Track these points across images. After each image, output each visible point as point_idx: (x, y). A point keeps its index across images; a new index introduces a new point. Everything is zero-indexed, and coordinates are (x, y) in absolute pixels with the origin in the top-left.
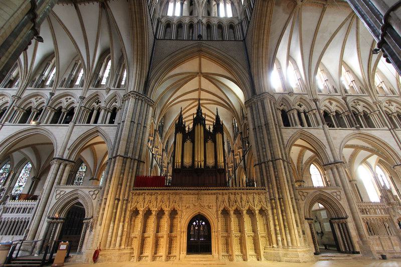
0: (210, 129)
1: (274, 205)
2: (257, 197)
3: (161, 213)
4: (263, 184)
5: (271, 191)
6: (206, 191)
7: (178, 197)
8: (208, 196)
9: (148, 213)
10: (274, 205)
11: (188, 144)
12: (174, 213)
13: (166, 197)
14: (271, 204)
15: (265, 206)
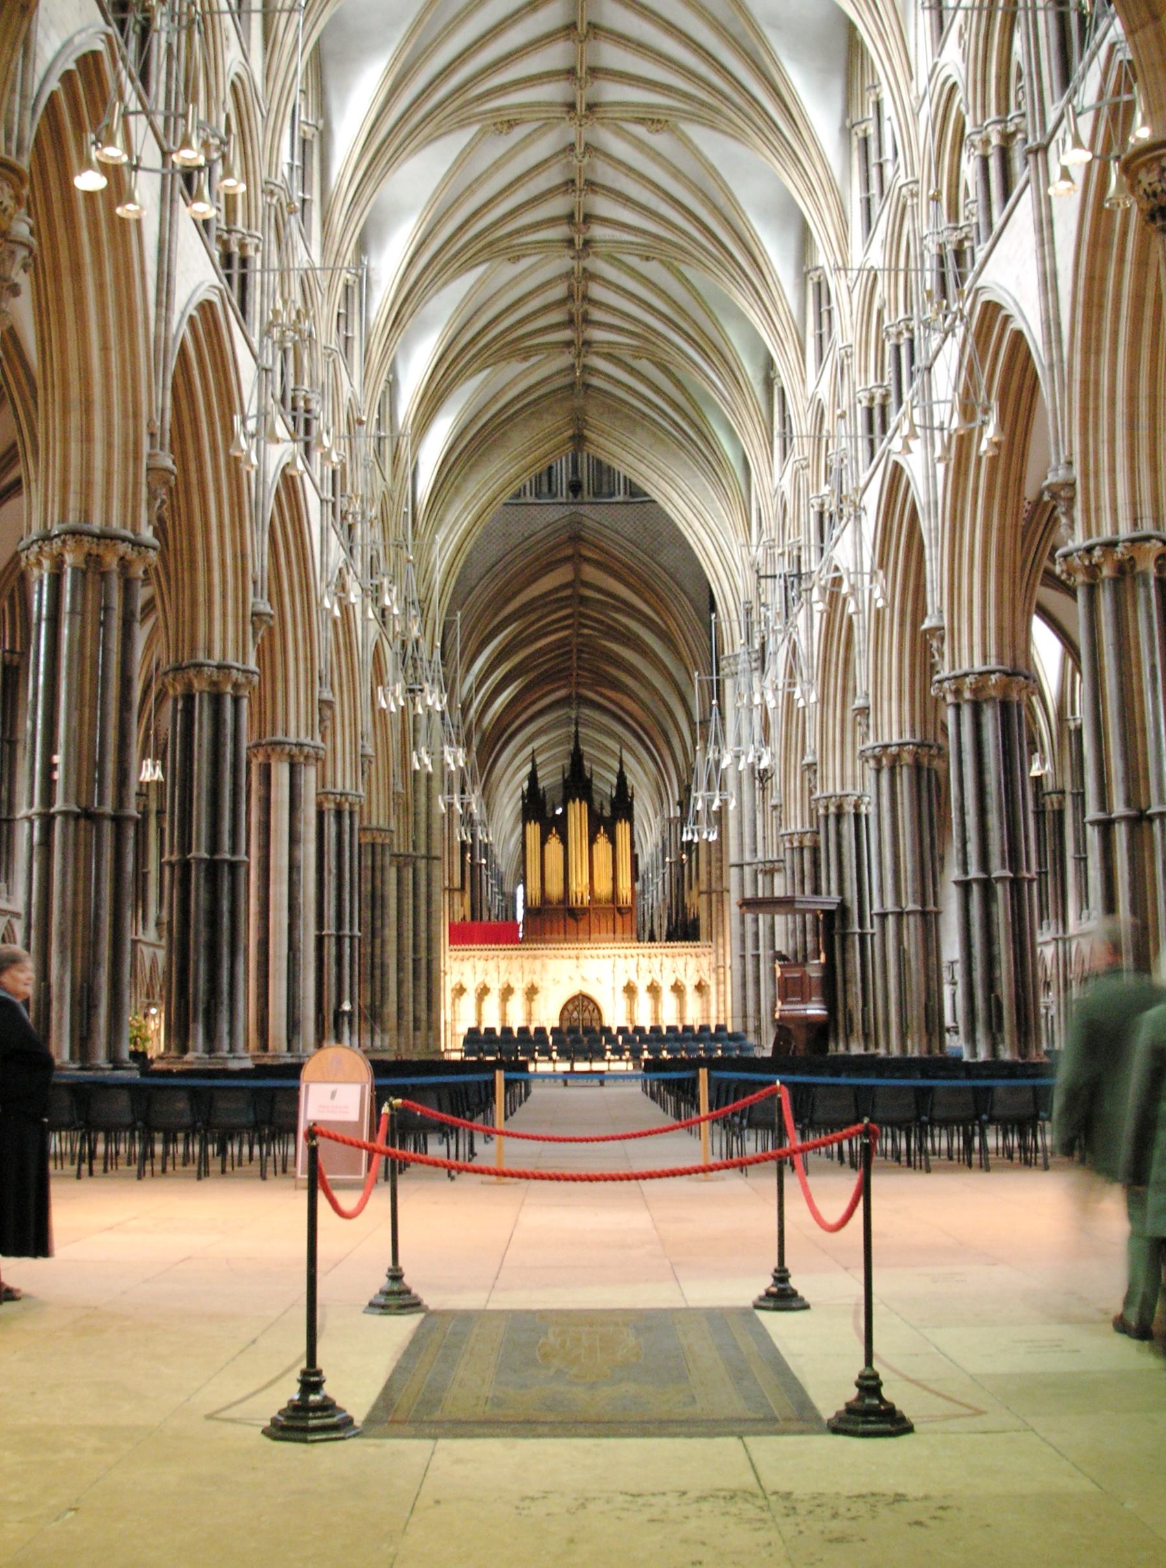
0: (602, 808)
1: (722, 977)
2: (692, 963)
3: (507, 992)
4: (710, 937)
5: (721, 951)
6: (593, 952)
7: (538, 963)
8: (596, 960)
9: (484, 991)
10: (722, 977)
11: (554, 845)
12: (532, 992)
13: (516, 964)
14: (717, 974)
15: (706, 978)
